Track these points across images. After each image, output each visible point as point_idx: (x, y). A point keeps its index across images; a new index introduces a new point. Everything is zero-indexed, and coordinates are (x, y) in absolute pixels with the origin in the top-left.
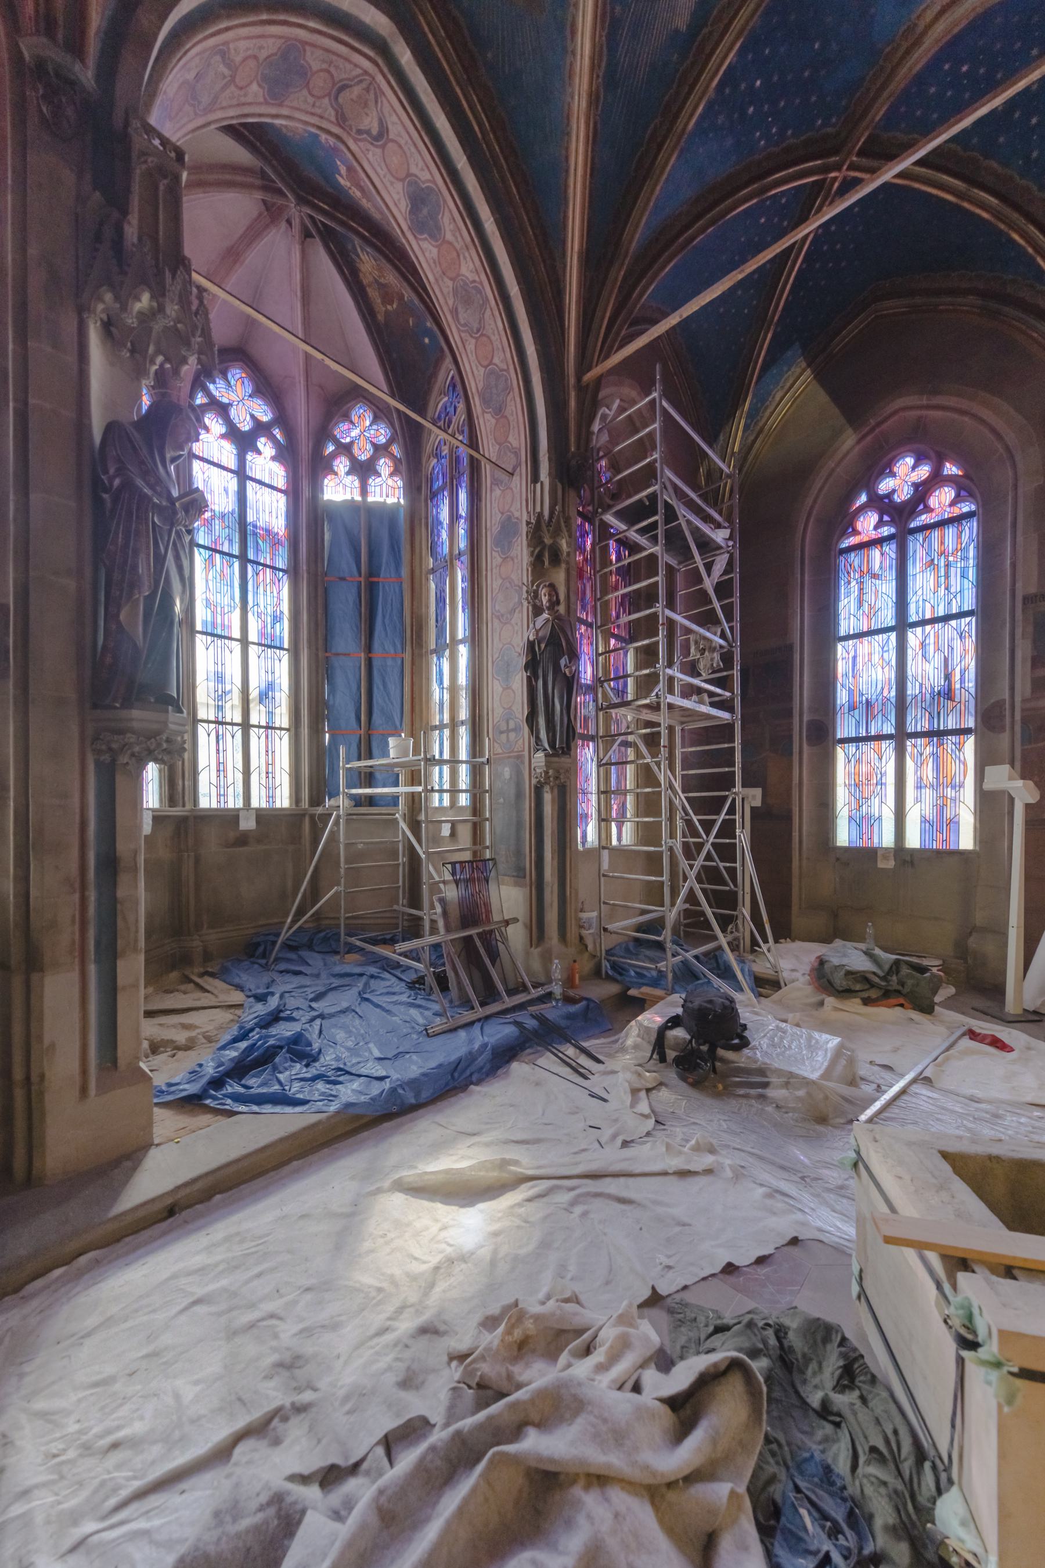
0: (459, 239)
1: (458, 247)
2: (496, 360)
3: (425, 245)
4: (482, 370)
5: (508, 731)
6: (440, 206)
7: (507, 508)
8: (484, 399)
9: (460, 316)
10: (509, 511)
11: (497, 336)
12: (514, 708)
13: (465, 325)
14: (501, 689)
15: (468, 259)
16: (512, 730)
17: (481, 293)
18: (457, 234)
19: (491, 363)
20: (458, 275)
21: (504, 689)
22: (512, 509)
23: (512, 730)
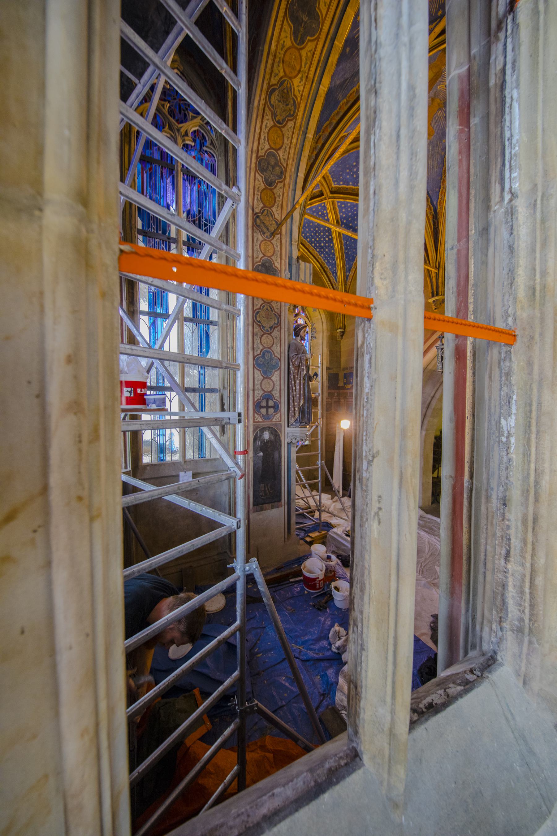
0: (308, 66)
1: (303, 68)
2: (281, 153)
3: (286, 27)
4: (267, 147)
5: (267, 407)
6: (314, 35)
7: (269, 255)
8: (260, 164)
9: (273, 97)
10: (270, 257)
11: (289, 142)
12: (273, 392)
13: (273, 106)
14: (262, 378)
15: (303, 82)
16: (271, 407)
17: (295, 109)
18: (309, 63)
19: (277, 150)
20: (291, 78)
21: (264, 378)
22: (273, 258)
23: (271, 407)
